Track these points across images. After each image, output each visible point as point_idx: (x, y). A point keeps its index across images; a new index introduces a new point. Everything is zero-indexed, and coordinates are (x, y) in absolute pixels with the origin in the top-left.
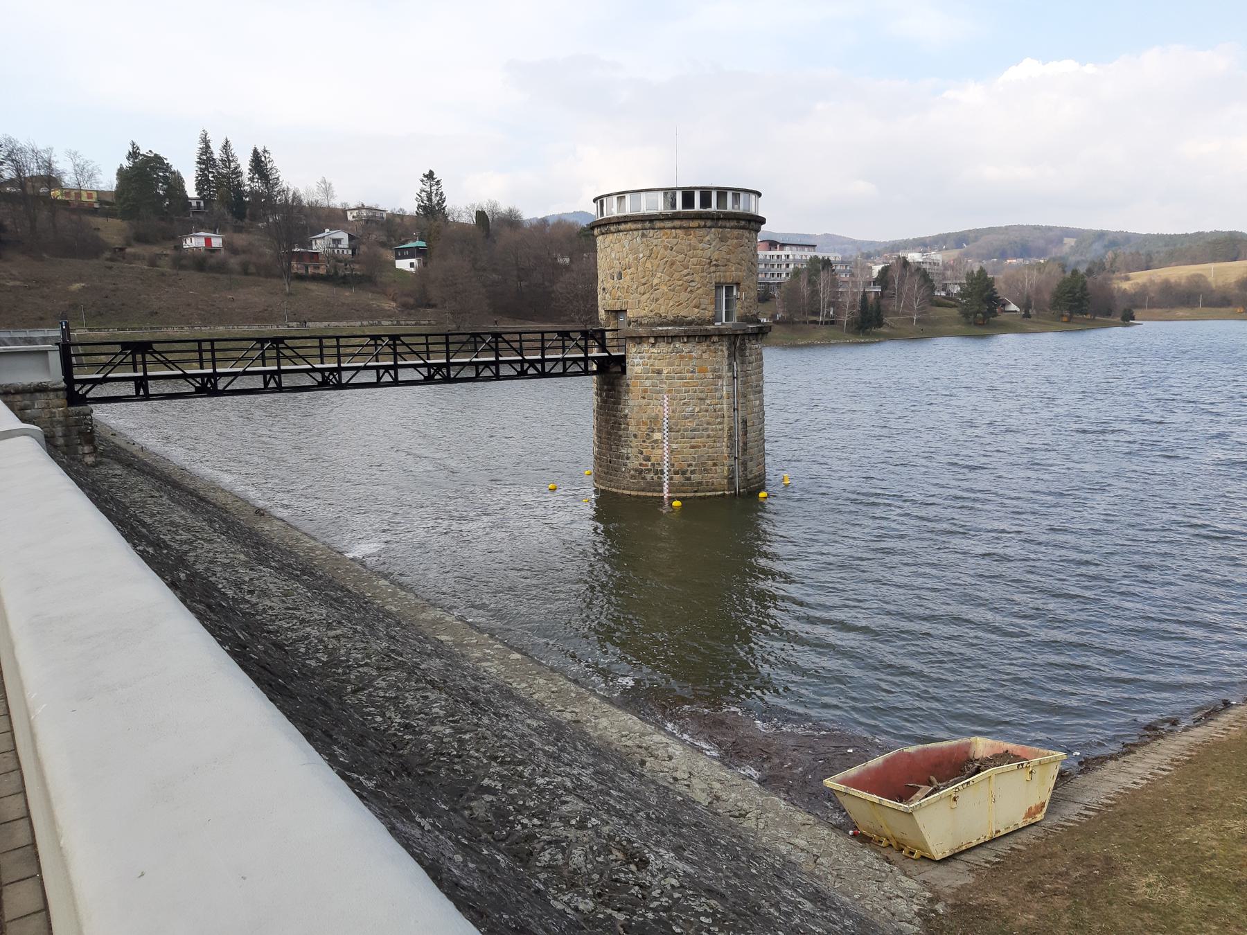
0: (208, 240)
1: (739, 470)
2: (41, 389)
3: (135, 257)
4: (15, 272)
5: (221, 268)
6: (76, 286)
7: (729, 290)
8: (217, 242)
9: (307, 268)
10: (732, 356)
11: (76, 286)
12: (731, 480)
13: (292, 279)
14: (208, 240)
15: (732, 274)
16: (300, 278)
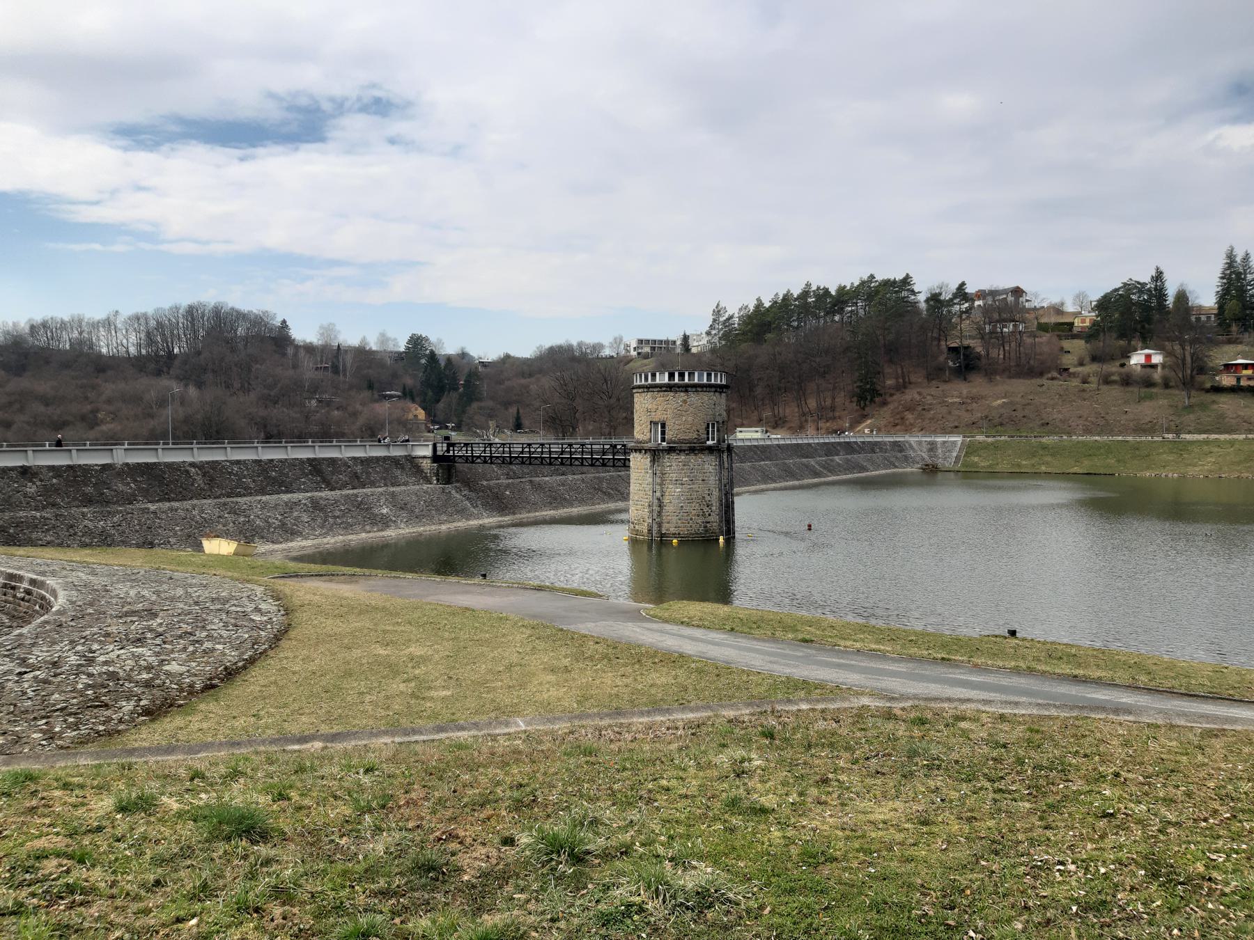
0: (1148, 357)
1: (655, 528)
2: (424, 457)
3: (1074, 375)
4: (965, 392)
5: (1149, 383)
6: (999, 402)
7: (663, 426)
8: (1157, 359)
9: (1239, 379)
10: (653, 461)
11: (999, 402)
12: (650, 531)
13: (1208, 391)
14: (1148, 357)
15: (658, 417)
16: (1218, 389)
